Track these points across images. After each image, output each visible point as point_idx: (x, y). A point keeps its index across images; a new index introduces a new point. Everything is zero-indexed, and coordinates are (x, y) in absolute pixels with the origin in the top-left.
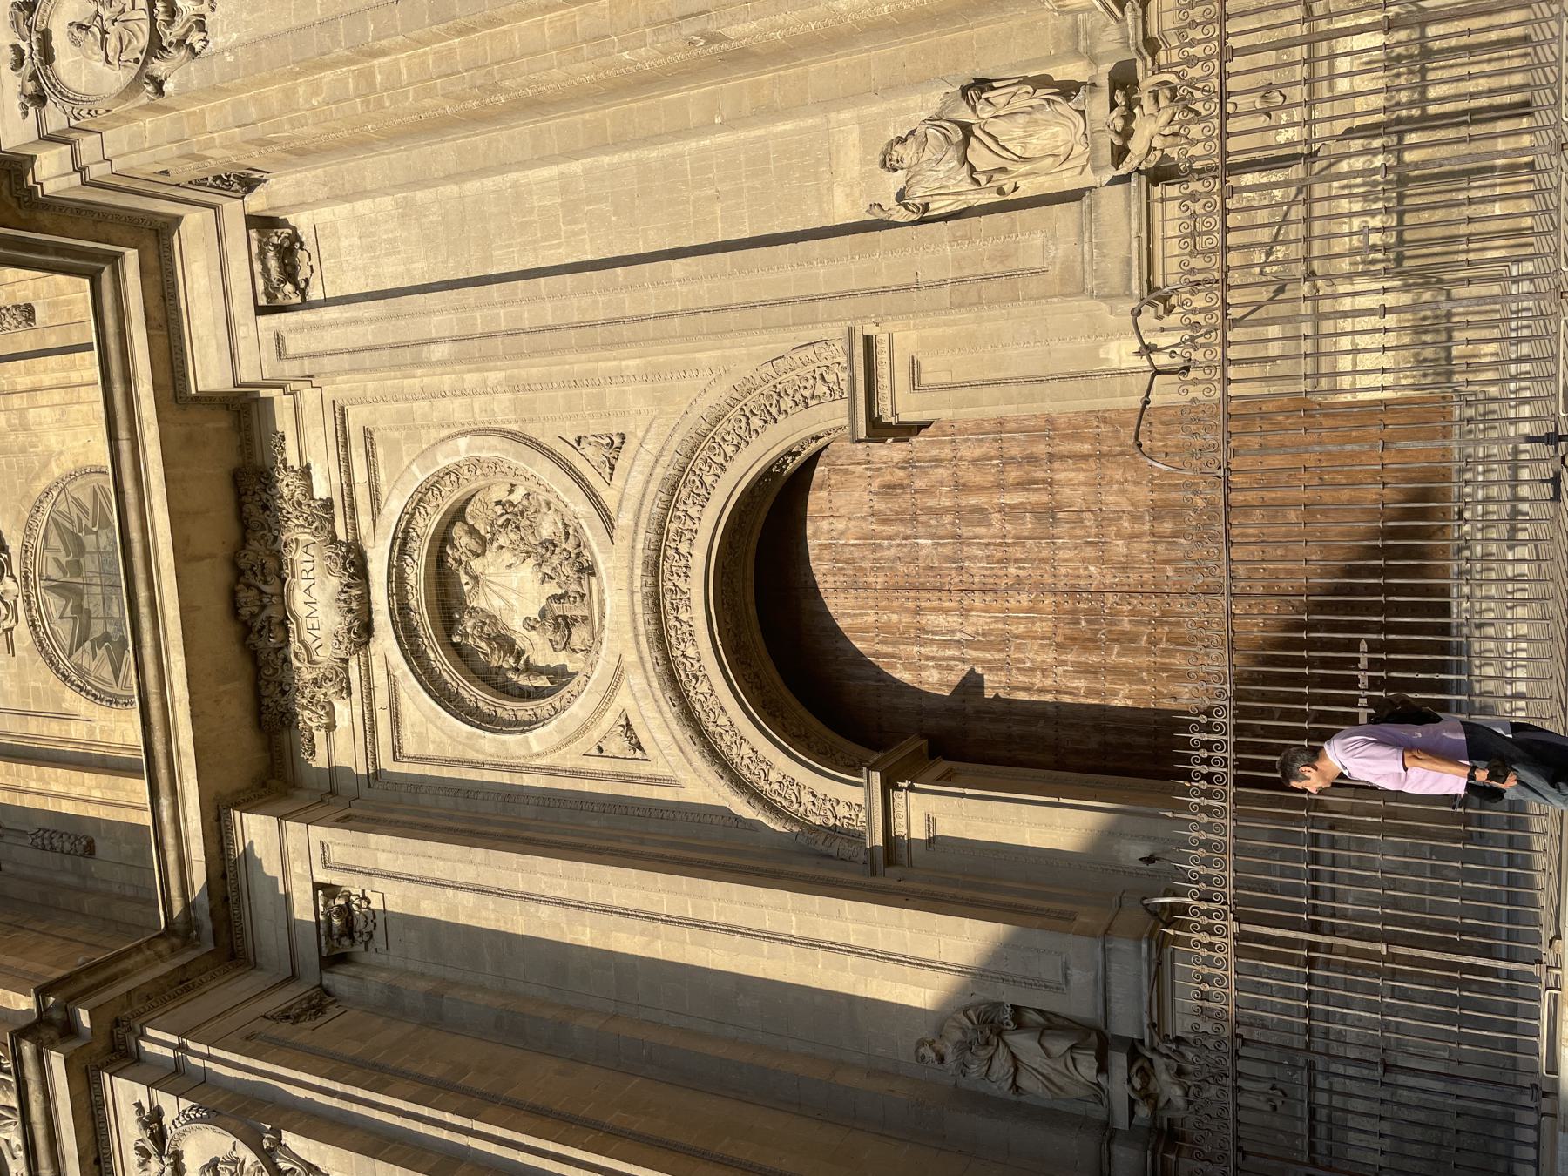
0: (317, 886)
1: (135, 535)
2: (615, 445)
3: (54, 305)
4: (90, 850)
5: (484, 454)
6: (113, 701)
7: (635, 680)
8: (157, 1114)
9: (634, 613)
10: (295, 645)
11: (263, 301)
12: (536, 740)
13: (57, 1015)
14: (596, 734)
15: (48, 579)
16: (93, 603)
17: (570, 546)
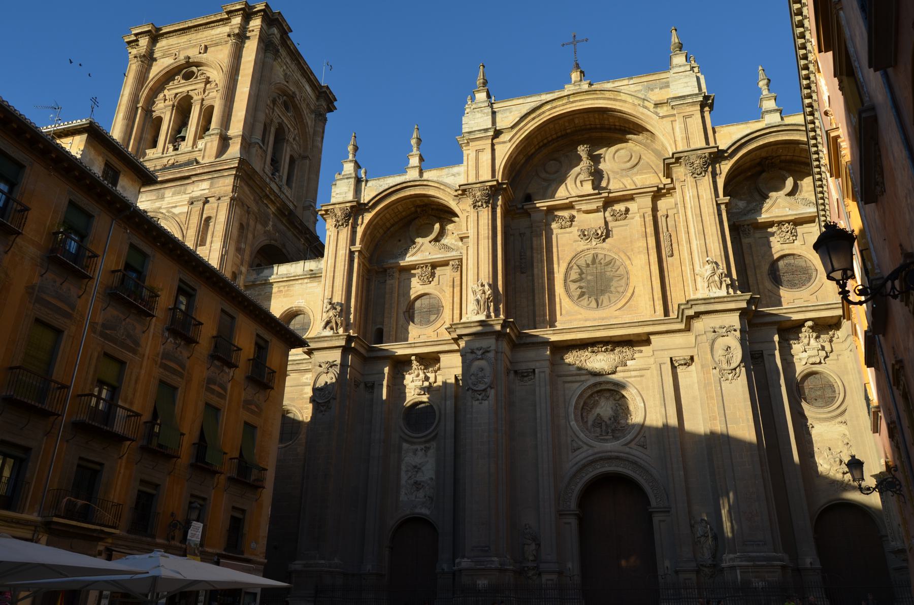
0: (534, 370)
1: (616, 326)
2: (643, 447)
3: (673, 265)
4: (522, 273)
5: (640, 411)
6: (565, 281)
7: (590, 452)
8: (488, 352)
9: (606, 452)
10: (589, 354)
11: (673, 359)
12: (573, 423)
13: (507, 324)
14: (576, 440)
15: (597, 256)
16: (592, 269)
17: (619, 428)
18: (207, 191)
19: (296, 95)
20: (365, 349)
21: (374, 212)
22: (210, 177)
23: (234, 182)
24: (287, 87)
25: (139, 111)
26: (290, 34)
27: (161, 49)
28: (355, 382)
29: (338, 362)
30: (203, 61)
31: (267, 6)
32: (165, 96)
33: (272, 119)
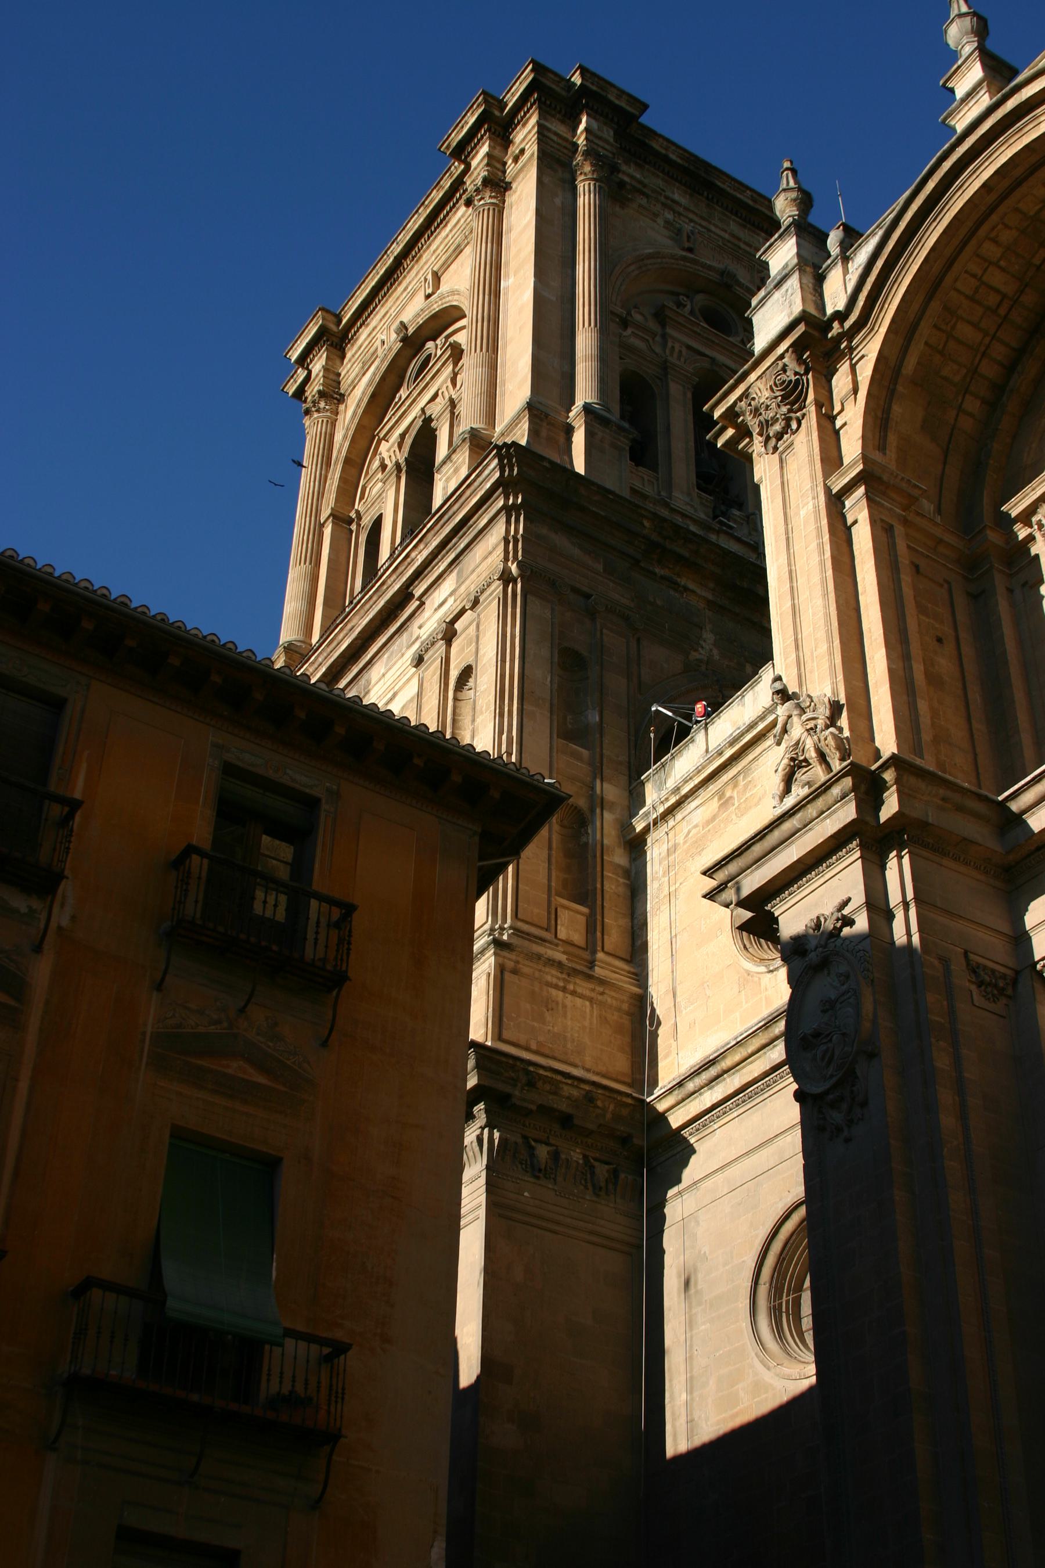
18: (451, 601)
19: (733, 276)
20: (977, 815)
21: (883, 330)
22: (452, 556)
23: (508, 531)
24: (695, 262)
25: (328, 531)
26: (643, 120)
27: (356, 356)
28: (974, 972)
29: (859, 897)
30: (436, 308)
31: (539, 68)
32: (382, 460)
33: (666, 361)
